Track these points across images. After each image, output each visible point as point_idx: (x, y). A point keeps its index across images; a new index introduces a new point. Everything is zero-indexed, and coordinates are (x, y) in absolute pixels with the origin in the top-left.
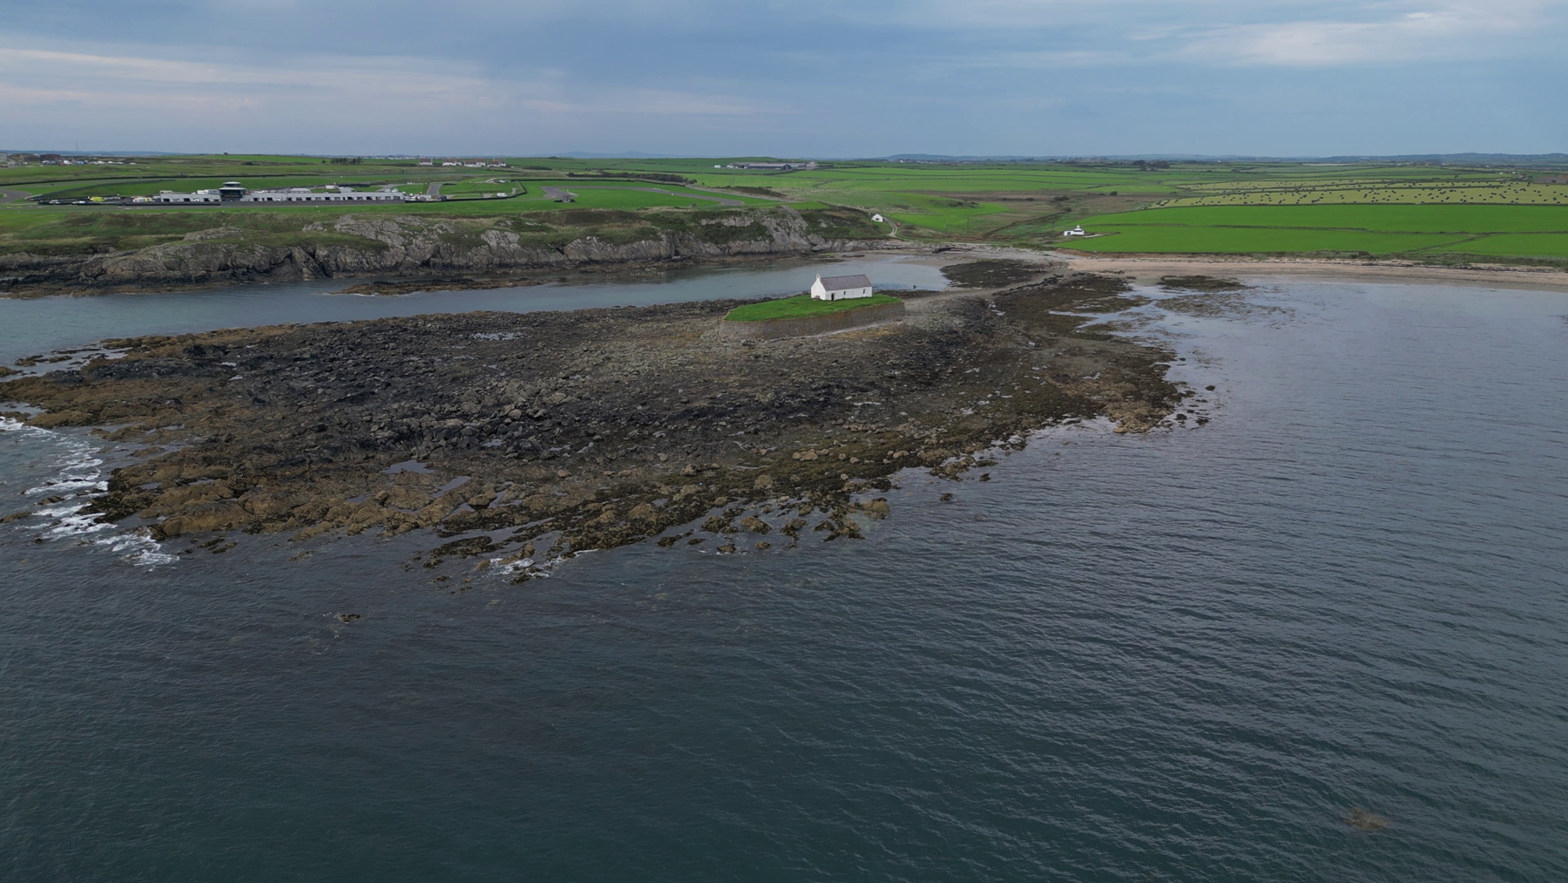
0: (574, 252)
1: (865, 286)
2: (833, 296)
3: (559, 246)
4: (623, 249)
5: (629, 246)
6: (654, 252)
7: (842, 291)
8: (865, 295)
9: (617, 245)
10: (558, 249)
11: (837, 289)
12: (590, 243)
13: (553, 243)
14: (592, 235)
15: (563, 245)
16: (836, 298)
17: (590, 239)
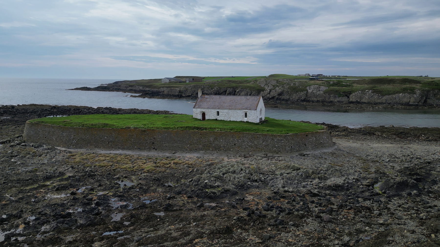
0: (353, 98)
1: (246, 109)
2: (204, 114)
3: (347, 94)
4: (385, 98)
5: (390, 96)
6: (405, 100)
7: (215, 111)
8: (245, 120)
9: (383, 95)
10: (347, 96)
11: (208, 108)
12: (366, 94)
13: (344, 92)
14: (370, 90)
15: (350, 94)
16: (207, 117)
17: (367, 91)
